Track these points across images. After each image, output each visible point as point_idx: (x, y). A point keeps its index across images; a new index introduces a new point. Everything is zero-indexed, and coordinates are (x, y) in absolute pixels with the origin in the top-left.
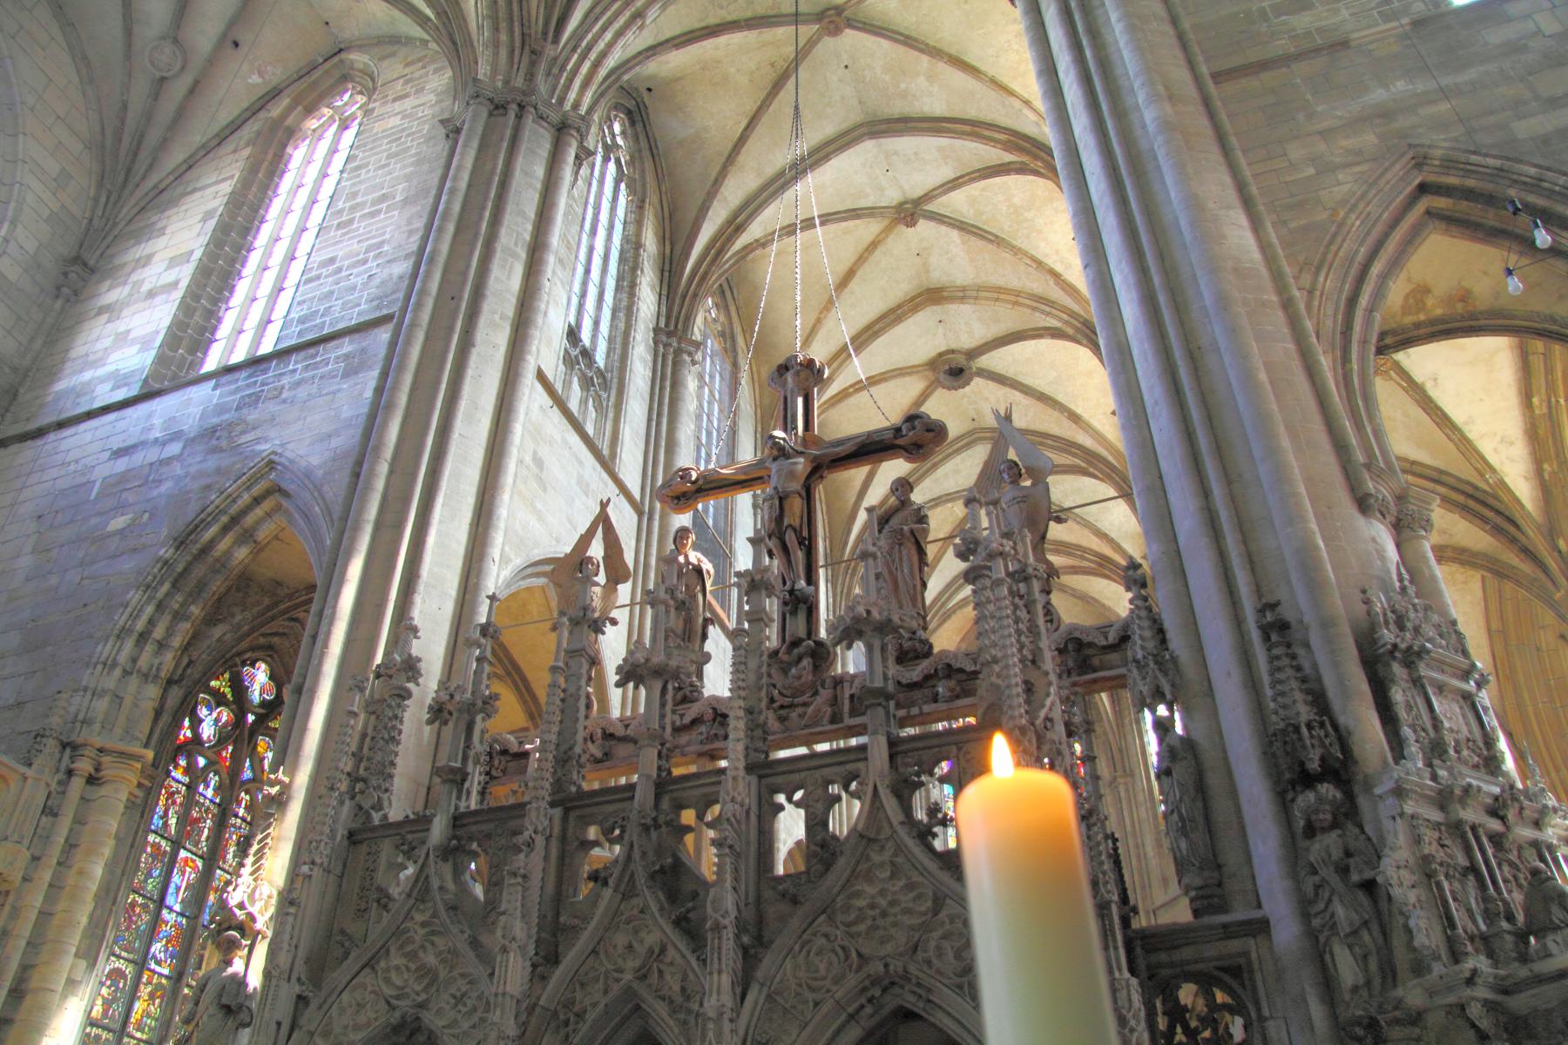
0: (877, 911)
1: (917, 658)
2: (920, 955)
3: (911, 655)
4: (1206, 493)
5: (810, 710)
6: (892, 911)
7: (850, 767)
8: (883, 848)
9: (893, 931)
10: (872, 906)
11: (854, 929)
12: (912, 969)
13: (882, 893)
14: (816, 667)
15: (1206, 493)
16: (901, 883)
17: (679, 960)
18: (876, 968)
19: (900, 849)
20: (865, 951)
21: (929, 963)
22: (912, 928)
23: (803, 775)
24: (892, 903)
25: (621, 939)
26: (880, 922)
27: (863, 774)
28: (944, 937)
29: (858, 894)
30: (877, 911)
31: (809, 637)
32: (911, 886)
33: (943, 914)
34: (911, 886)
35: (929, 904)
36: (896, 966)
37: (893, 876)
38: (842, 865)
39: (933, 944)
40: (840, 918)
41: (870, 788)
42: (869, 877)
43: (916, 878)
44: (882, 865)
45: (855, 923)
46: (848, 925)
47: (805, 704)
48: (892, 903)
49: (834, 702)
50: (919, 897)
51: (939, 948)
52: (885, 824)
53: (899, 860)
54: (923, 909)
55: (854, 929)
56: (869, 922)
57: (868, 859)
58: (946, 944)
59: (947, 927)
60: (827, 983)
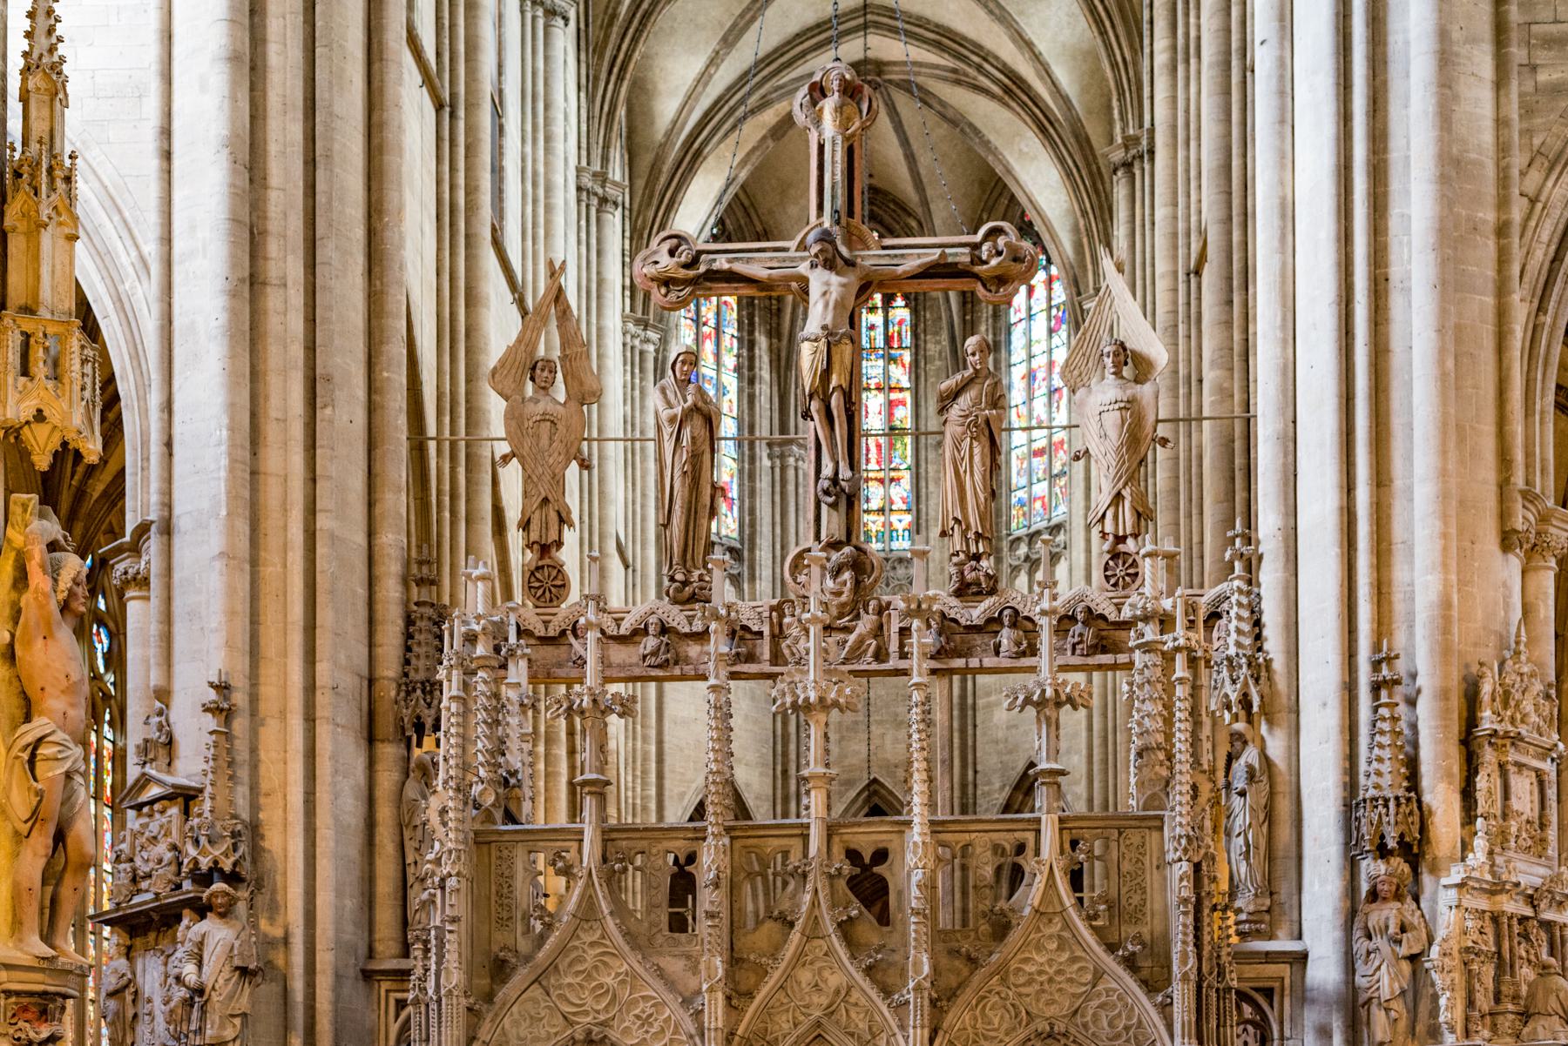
0: (1044, 978)
1: (979, 593)
2: (1079, 1020)
3: (974, 589)
4: (1349, 488)
5: (852, 638)
6: (1058, 979)
7: (1017, 835)
8: (1050, 921)
9: (1056, 997)
10: (1040, 973)
11: (1023, 990)
12: (1072, 1030)
13: (1050, 962)
14: (857, 583)
15: (1349, 488)
16: (1066, 955)
17: (863, 1001)
18: (1043, 1026)
19: (1067, 925)
20: (1034, 1011)
21: (1085, 1026)
22: (1074, 995)
23: (974, 835)
24: (1059, 972)
25: (805, 976)
26: (1046, 986)
27: (1031, 845)
28: (1101, 1006)
29: (1026, 960)
30: (1044, 978)
31: (848, 542)
32: (1074, 960)
33: (1100, 987)
34: (1074, 960)
35: (1089, 977)
36: (1060, 1027)
37: (1060, 948)
38: (1015, 936)
39: (1091, 1012)
40: (1012, 978)
41: (1046, 870)
42: (1039, 948)
43: (1079, 953)
44: (1051, 937)
45: (1023, 985)
46: (1016, 986)
47: (848, 630)
48: (1059, 972)
49: (879, 631)
50: (1081, 969)
51: (1094, 1015)
52: (1056, 901)
53: (1066, 934)
54: (1083, 980)
55: (1023, 990)
56: (1037, 987)
57: (1039, 930)
58: (1103, 1014)
59: (1103, 999)
60: (1001, 1036)
